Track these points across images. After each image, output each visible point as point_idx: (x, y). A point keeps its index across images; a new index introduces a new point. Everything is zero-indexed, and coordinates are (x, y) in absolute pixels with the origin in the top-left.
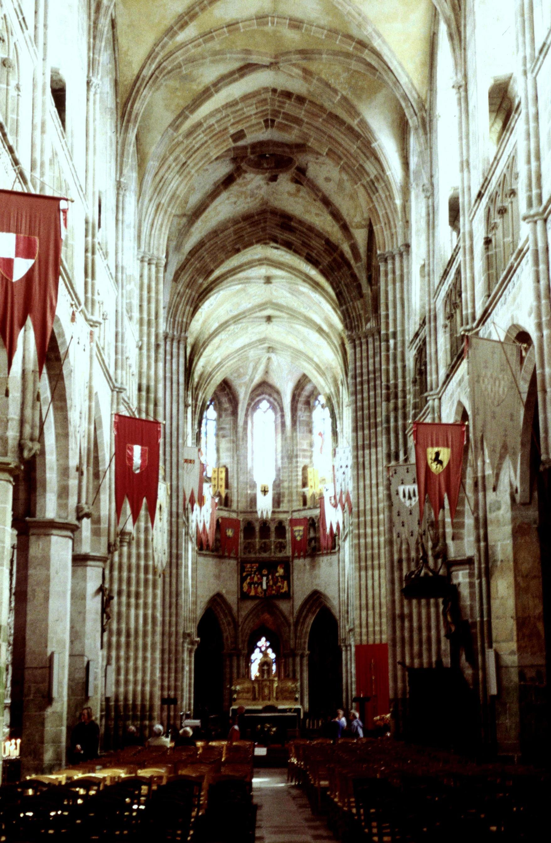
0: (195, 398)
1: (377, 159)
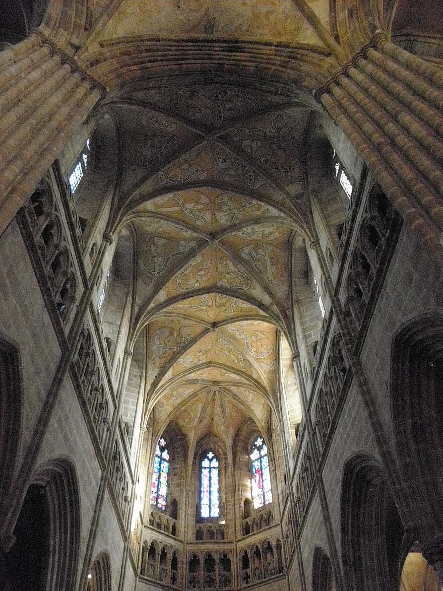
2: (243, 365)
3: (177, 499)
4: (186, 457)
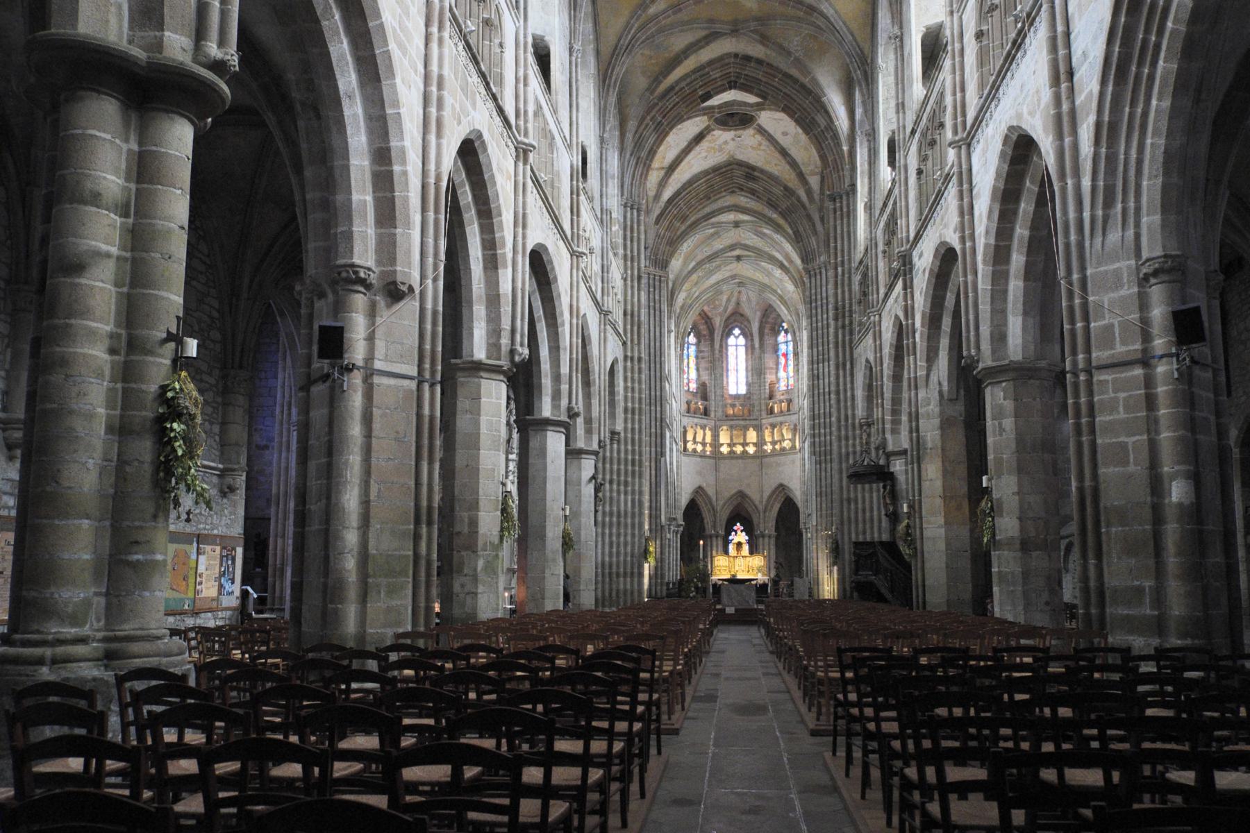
0: (677, 326)
1: (827, 112)
4: (712, 340)
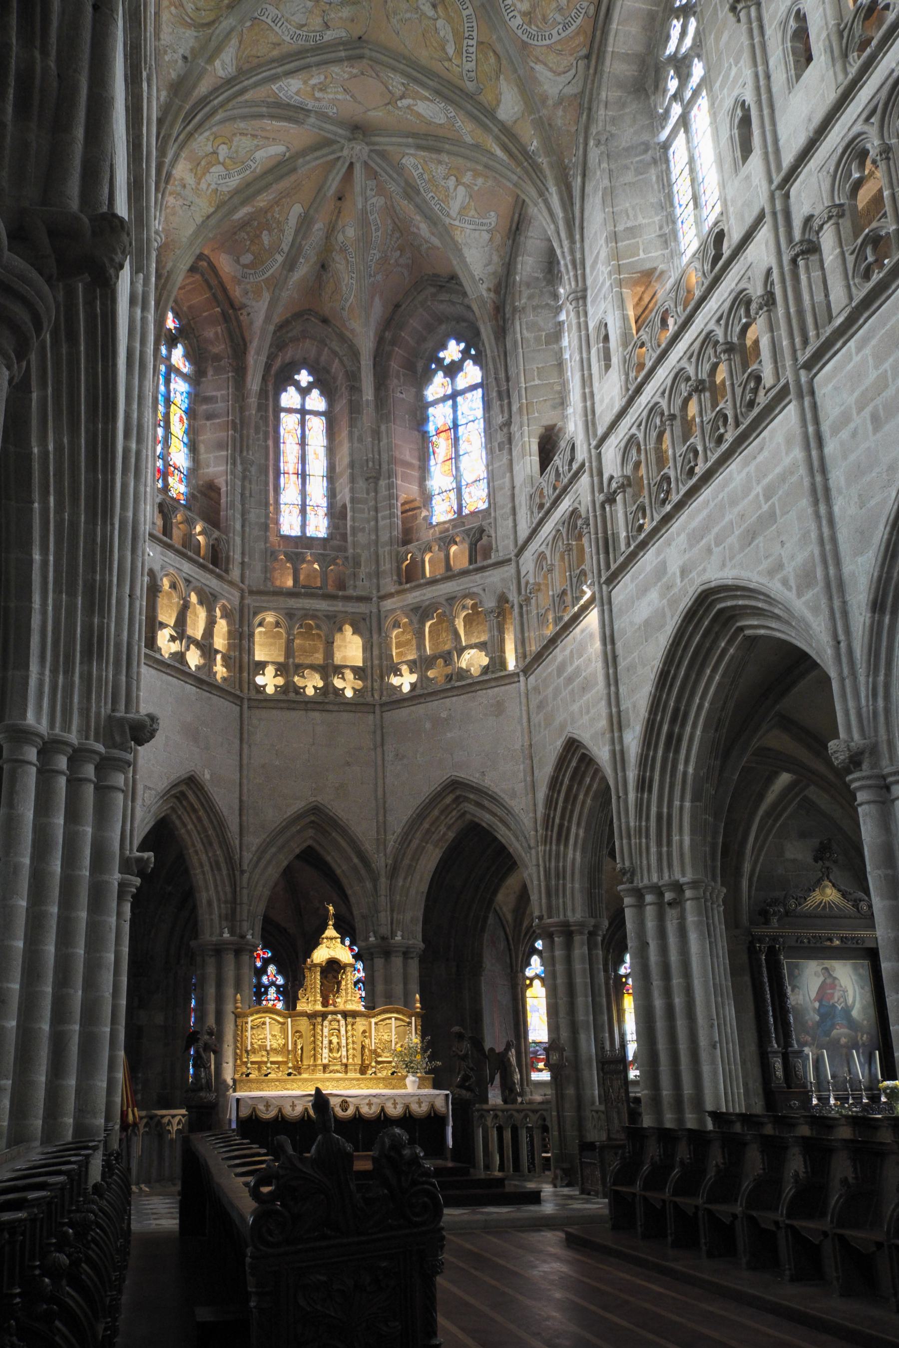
2: (471, 65)
3: (221, 482)
4: (240, 372)
